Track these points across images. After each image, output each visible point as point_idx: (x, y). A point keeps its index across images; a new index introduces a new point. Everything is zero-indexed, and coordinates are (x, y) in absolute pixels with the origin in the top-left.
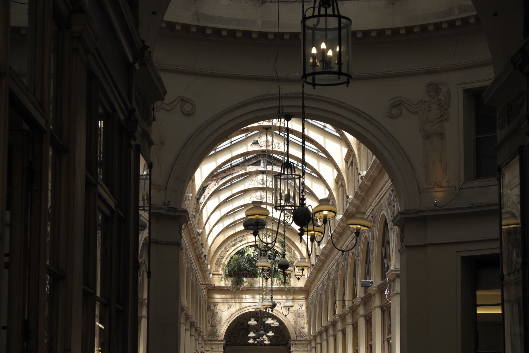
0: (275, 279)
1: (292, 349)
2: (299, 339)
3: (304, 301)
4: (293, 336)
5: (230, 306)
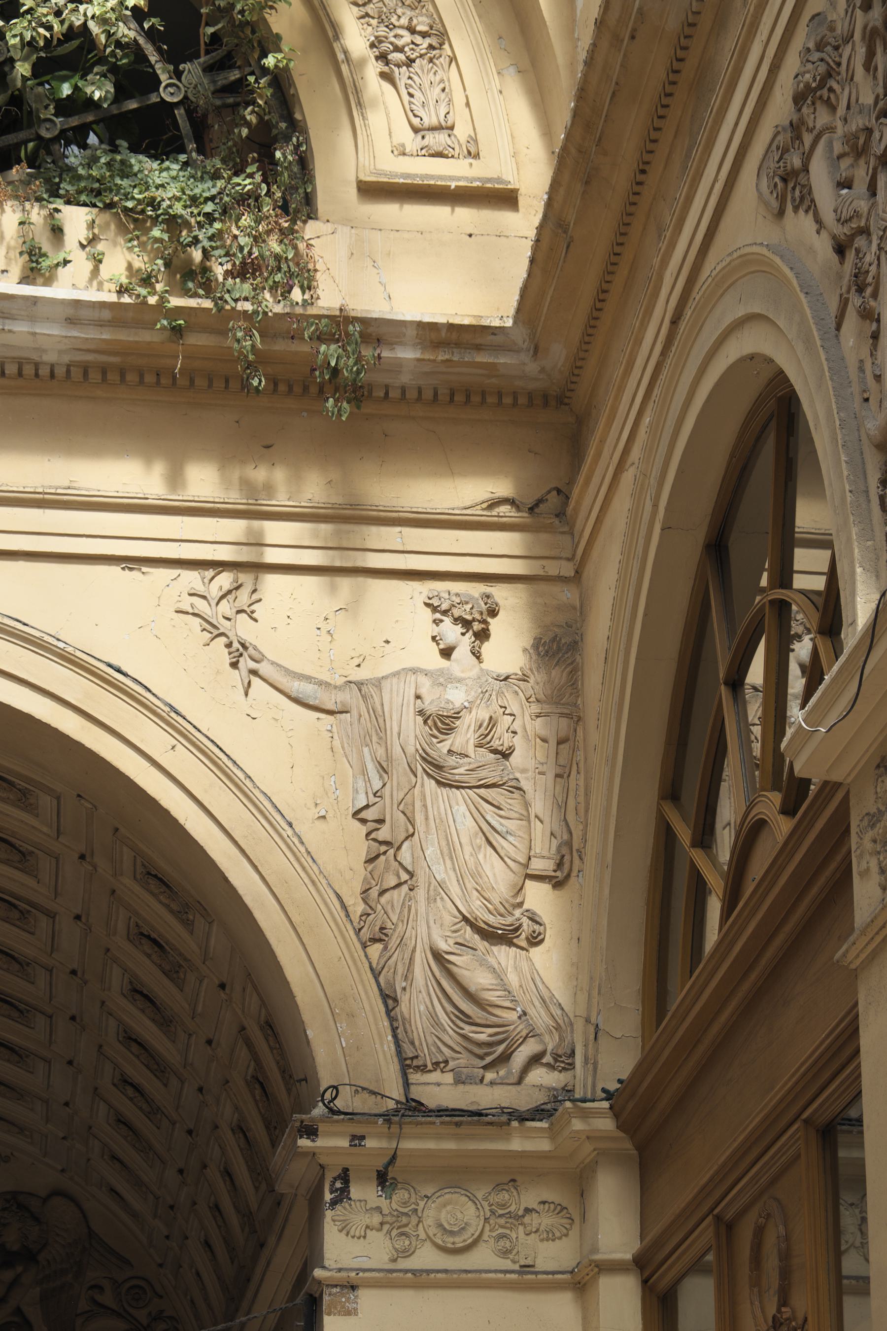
0: (76, 220)
1: (347, 1244)
2: (438, 1090)
3: (500, 549)
4: (343, 1042)
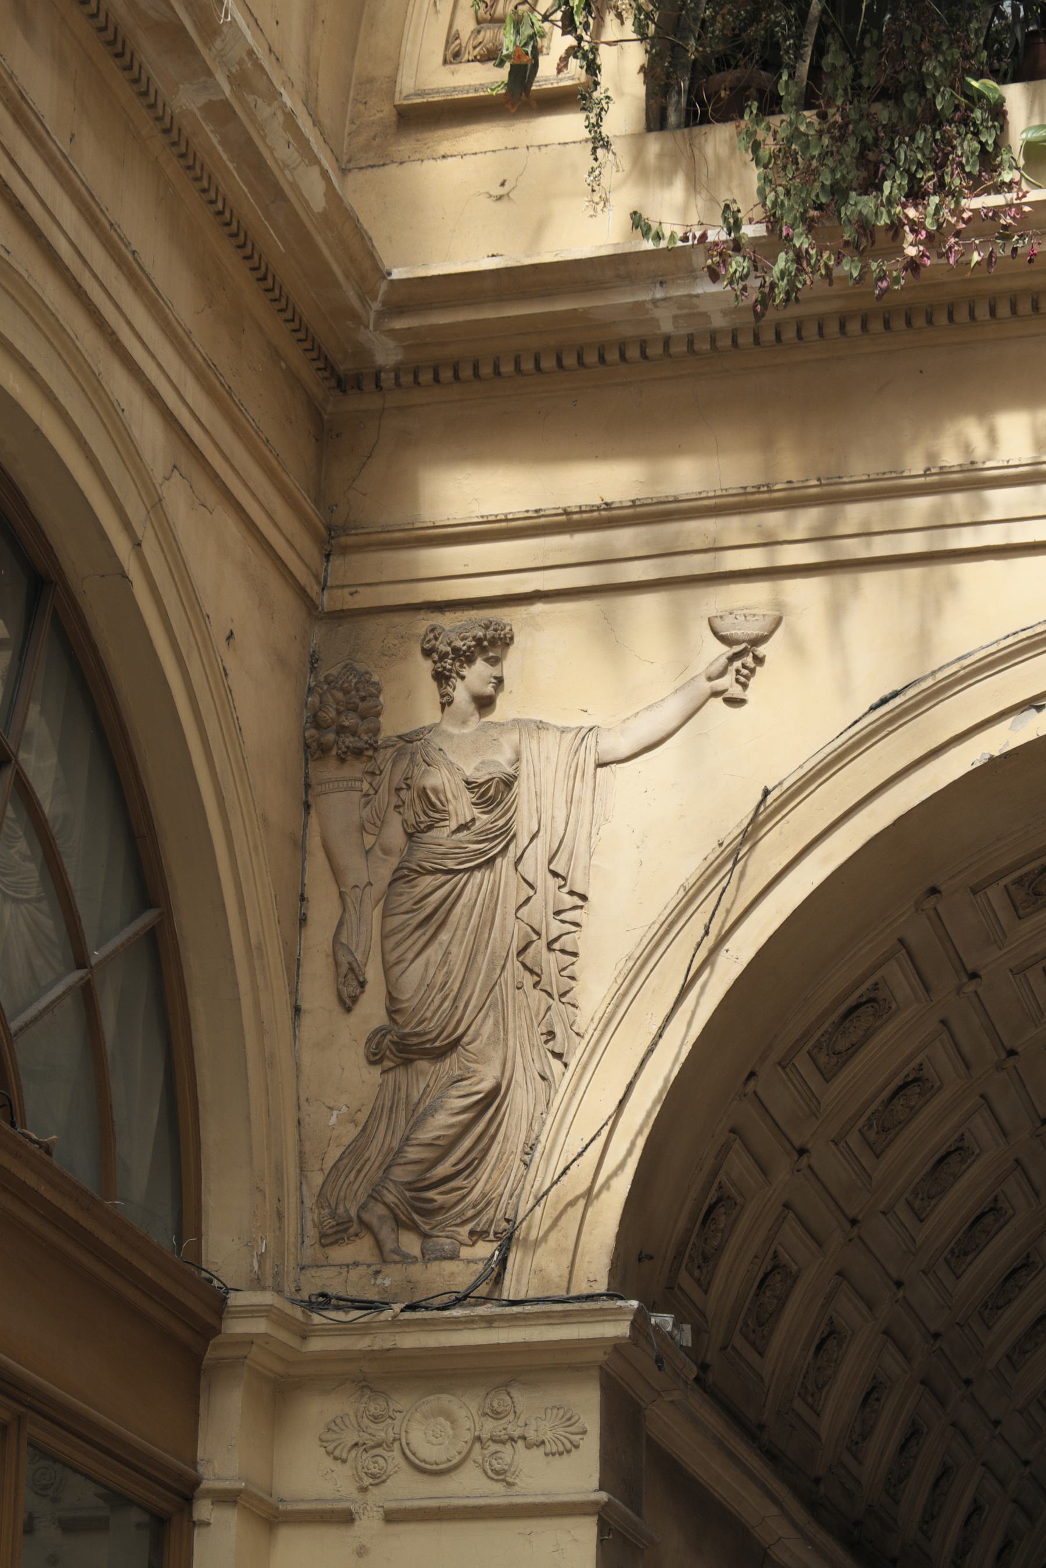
5: (745, 653)
